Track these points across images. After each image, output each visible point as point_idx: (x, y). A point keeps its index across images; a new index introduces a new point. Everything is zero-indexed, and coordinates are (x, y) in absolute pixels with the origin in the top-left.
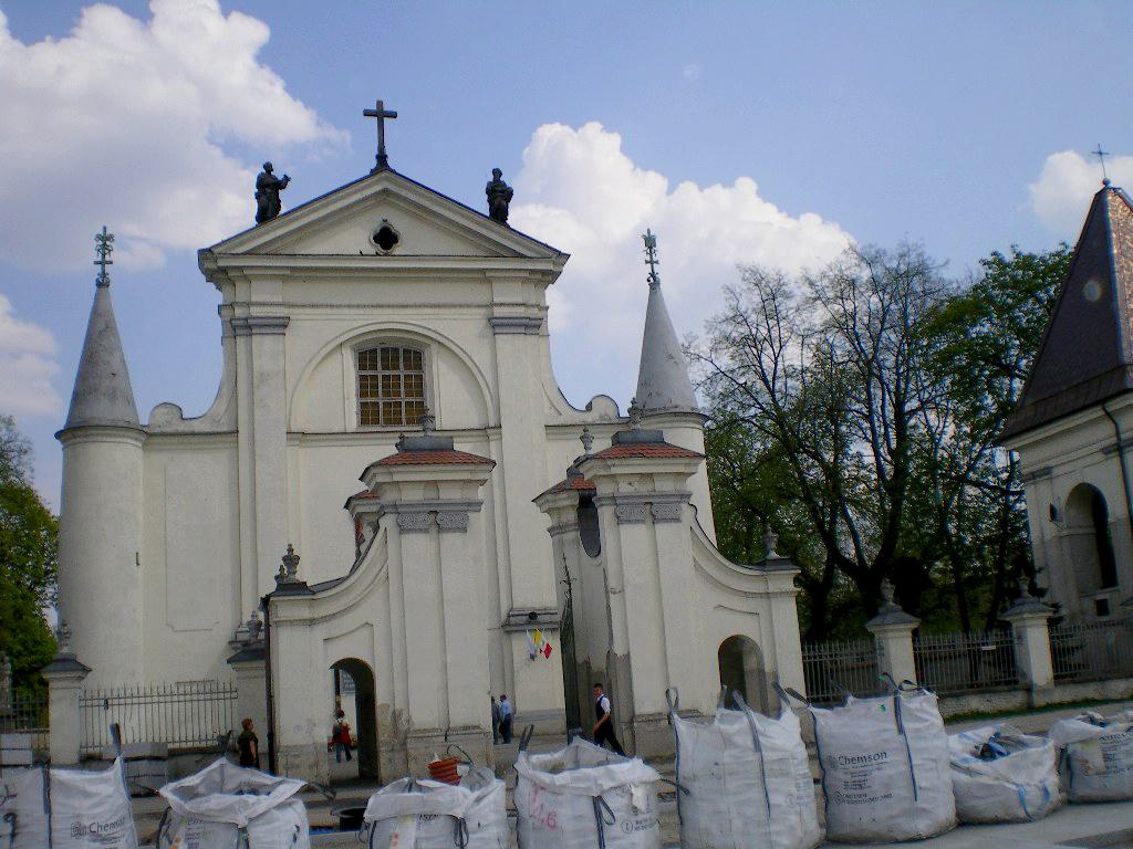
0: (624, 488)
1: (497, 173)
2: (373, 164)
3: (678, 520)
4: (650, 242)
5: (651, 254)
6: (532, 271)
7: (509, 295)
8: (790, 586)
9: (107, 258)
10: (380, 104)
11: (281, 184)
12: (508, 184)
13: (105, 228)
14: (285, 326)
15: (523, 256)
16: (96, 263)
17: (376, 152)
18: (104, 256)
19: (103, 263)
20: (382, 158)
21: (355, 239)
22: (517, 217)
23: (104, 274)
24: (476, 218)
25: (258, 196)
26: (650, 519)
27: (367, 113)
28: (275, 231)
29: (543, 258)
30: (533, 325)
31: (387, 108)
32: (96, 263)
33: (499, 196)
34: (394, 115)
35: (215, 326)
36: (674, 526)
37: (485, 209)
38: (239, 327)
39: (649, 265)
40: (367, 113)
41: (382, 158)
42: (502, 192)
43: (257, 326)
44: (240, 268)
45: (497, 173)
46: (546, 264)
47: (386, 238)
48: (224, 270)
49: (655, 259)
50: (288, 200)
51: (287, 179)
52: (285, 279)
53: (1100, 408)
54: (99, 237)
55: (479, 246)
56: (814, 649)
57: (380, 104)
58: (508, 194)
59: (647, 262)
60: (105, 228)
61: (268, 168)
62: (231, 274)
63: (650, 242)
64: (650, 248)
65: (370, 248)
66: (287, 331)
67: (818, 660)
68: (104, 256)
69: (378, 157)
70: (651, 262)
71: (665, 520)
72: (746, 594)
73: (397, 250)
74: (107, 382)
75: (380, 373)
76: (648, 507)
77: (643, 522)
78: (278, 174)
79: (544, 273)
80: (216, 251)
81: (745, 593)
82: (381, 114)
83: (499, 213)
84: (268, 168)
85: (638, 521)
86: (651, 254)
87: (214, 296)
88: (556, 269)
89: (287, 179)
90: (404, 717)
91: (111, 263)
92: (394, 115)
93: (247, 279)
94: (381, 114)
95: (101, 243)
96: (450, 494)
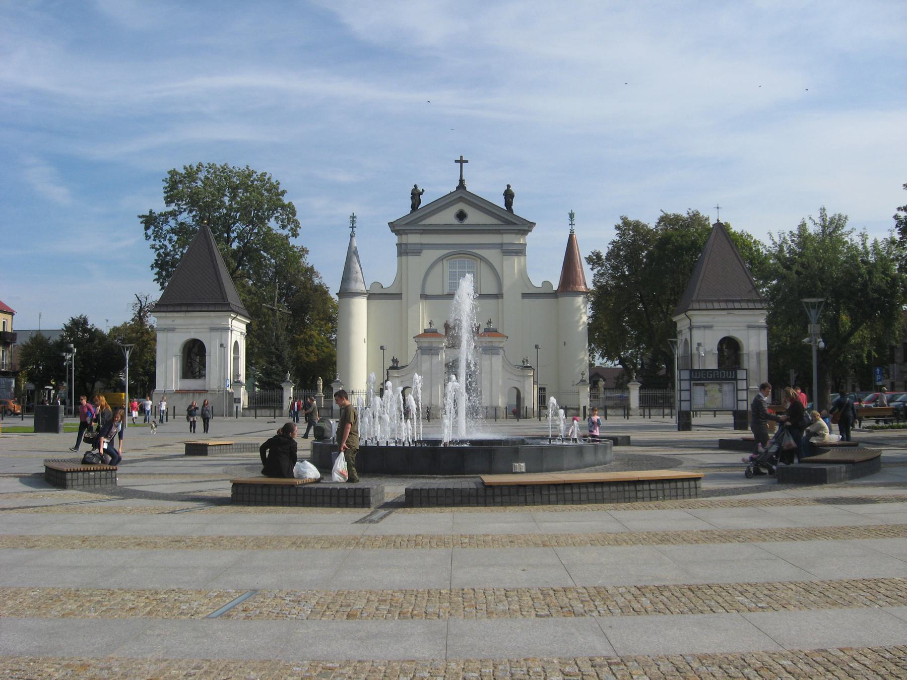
1: (509, 186)
2: (458, 184)
3: (498, 354)
4: (572, 216)
5: (572, 221)
6: (519, 230)
7: (508, 239)
9: (354, 225)
10: (461, 157)
14: (420, 253)
15: (515, 224)
17: (459, 178)
19: (353, 227)
20: (462, 181)
21: (448, 217)
23: (353, 232)
27: (456, 161)
28: (417, 215)
30: (520, 251)
33: (509, 196)
34: (467, 162)
35: (395, 250)
37: (501, 203)
38: (403, 250)
40: (456, 161)
41: (462, 181)
43: (410, 252)
44: (404, 230)
45: (509, 186)
46: (526, 227)
47: (461, 216)
50: (425, 201)
52: (422, 234)
53: (684, 314)
55: (501, 220)
57: (461, 157)
61: (415, 186)
62: (400, 232)
63: (572, 216)
65: (456, 222)
70: (571, 224)
72: (518, 376)
73: (466, 222)
74: (354, 275)
75: (457, 270)
77: (489, 354)
78: (420, 189)
79: (524, 230)
80: (395, 224)
82: (461, 161)
83: (509, 204)
84: (415, 186)
86: (572, 221)
87: (394, 238)
92: (467, 162)
93: (407, 234)
94: (461, 161)
96: (434, 345)
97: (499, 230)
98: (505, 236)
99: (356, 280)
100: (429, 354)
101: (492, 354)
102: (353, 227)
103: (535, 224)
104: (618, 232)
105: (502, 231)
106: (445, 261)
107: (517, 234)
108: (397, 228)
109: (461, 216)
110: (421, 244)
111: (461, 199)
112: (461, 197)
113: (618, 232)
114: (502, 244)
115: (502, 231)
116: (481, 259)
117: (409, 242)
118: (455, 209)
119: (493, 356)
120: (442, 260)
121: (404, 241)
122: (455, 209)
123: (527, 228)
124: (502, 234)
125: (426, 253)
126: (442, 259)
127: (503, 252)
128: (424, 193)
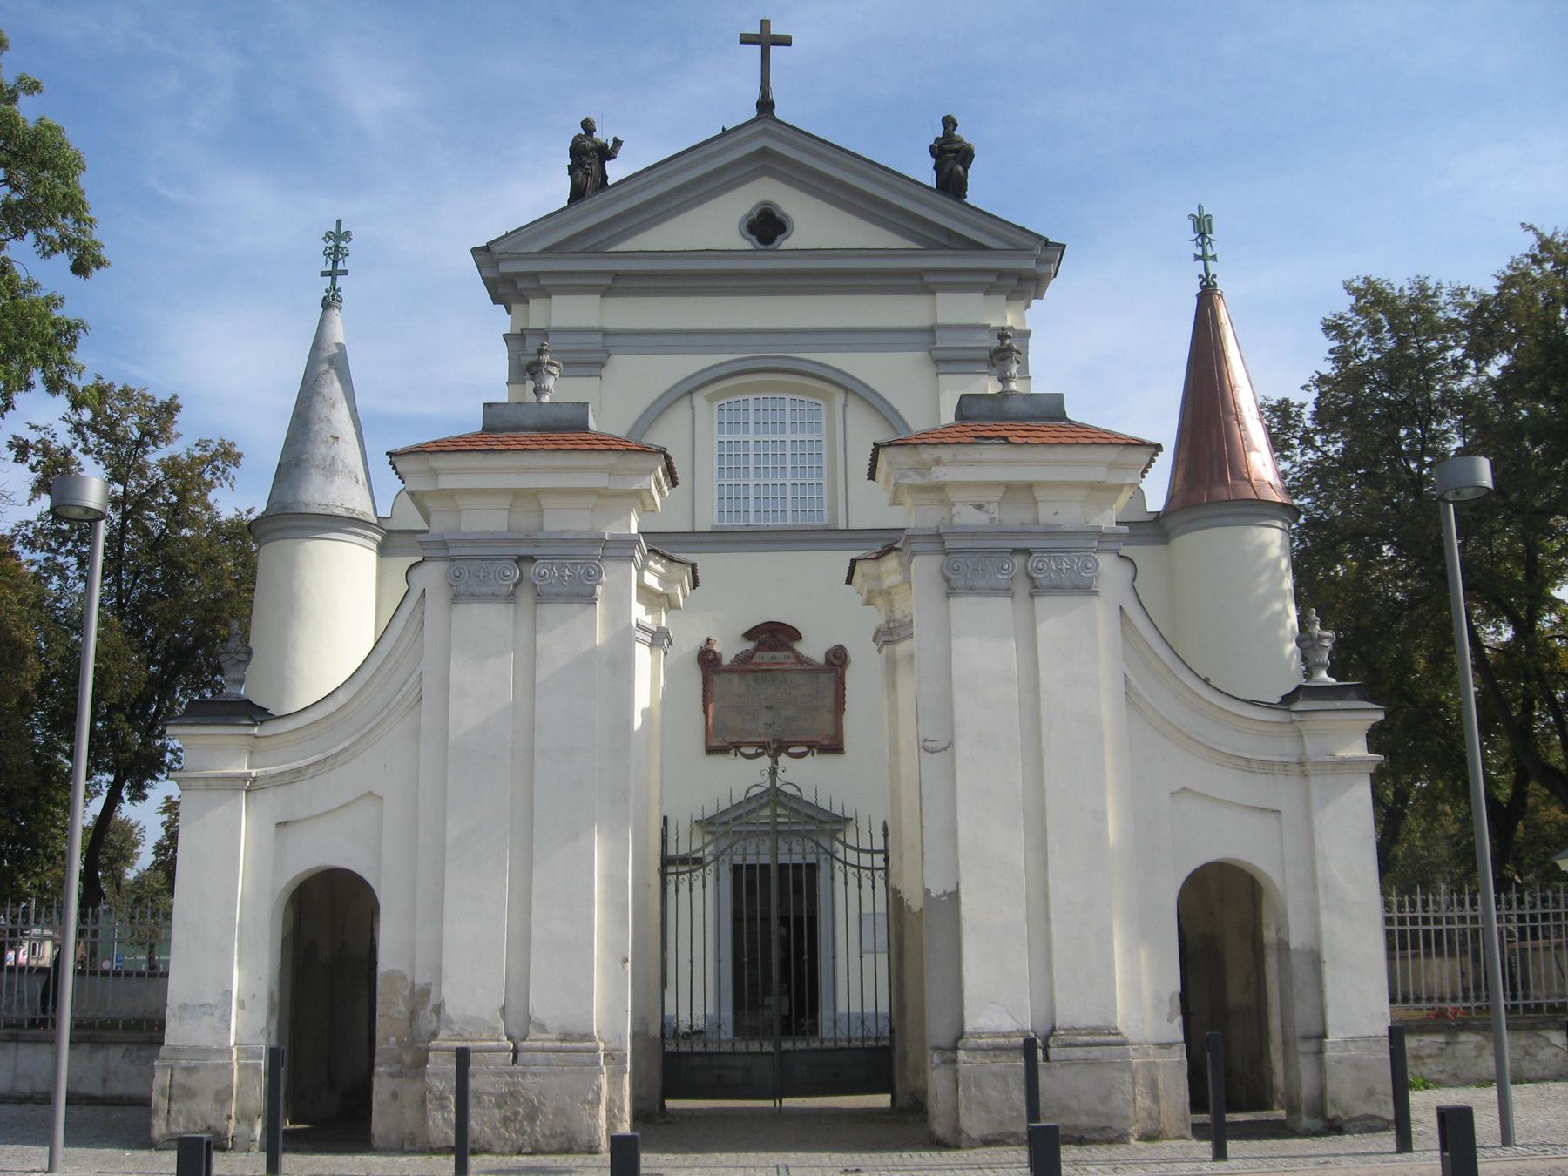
0: (966, 516)
1: (949, 123)
4: (1202, 227)
6: (1001, 274)
8: (1358, 750)
9: (340, 266)
10: (765, 24)
11: (606, 153)
12: (967, 140)
13: (339, 222)
14: (602, 365)
16: (323, 274)
17: (757, 96)
18: (335, 263)
19: (332, 274)
20: (765, 105)
22: (981, 189)
24: (914, 191)
25: (572, 170)
26: (1022, 588)
27: (746, 40)
29: (1018, 250)
31: (775, 30)
32: (323, 274)
34: (786, 41)
36: (1077, 607)
37: (929, 178)
39: (1201, 262)
40: (746, 40)
41: (765, 105)
42: (957, 151)
44: (535, 276)
45: (949, 123)
47: (767, 226)
48: (510, 280)
49: (1210, 253)
51: (618, 143)
52: (607, 292)
54: (328, 236)
55: (917, 242)
56: (1413, 904)
57: (765, 24)
58: (965, 155)
59: (1197, 258)
60: (339, 222)
61: (588, 126)
63: (1202, 227)
64: (1202, 235)
66: (604, 372)
67: (1444, 926)
68: (335, 263)
69: (759, 105)
70: (1202, 258)
71: (1057, 589)
72: (1249, 765)
74: (323, 449)
76: (1018, 561)
77: (1008, 591)
80: (497, 249)
81: (1248, 760)
82: (766, 40)
84: (588, 126)
85: (994, 591)
87: (501, 321)
88: (1042, 269)
89: (618, 143)
90: (433, 1001)
91: (345, 273)
92: (786, 41)
93: (546, 293)
94: (766, 40)
95: (331, 243)
96: (563, 520)
97: (918, 274)
98: (941, 297)
99: (330, 469)
100: (511, 598)
101: (1036, 589)
102: (332, 274)
103: (1064, 246)
104: (1336, 343)
105: (928, 279)
106: (700, 399)
107: (989, 290)
108: (506, 268)
109: (767, 226)
110: (605, 333)
111: (765, 163)
112: (764, 153)
113: (1336, 343)
114: (932, 330)
115: (928, 279)
116: (847, 390)
117: (557, 322)
118: (741, 202)
119: (1042, 603)
120: (690, 393)
121: (536, 322)
122: (741, 202)
123: (1030, 265)
124: (930, 291)
125: (622, 366)
126: (687, 390)
127: (937, 362)
128: (622, 151)
